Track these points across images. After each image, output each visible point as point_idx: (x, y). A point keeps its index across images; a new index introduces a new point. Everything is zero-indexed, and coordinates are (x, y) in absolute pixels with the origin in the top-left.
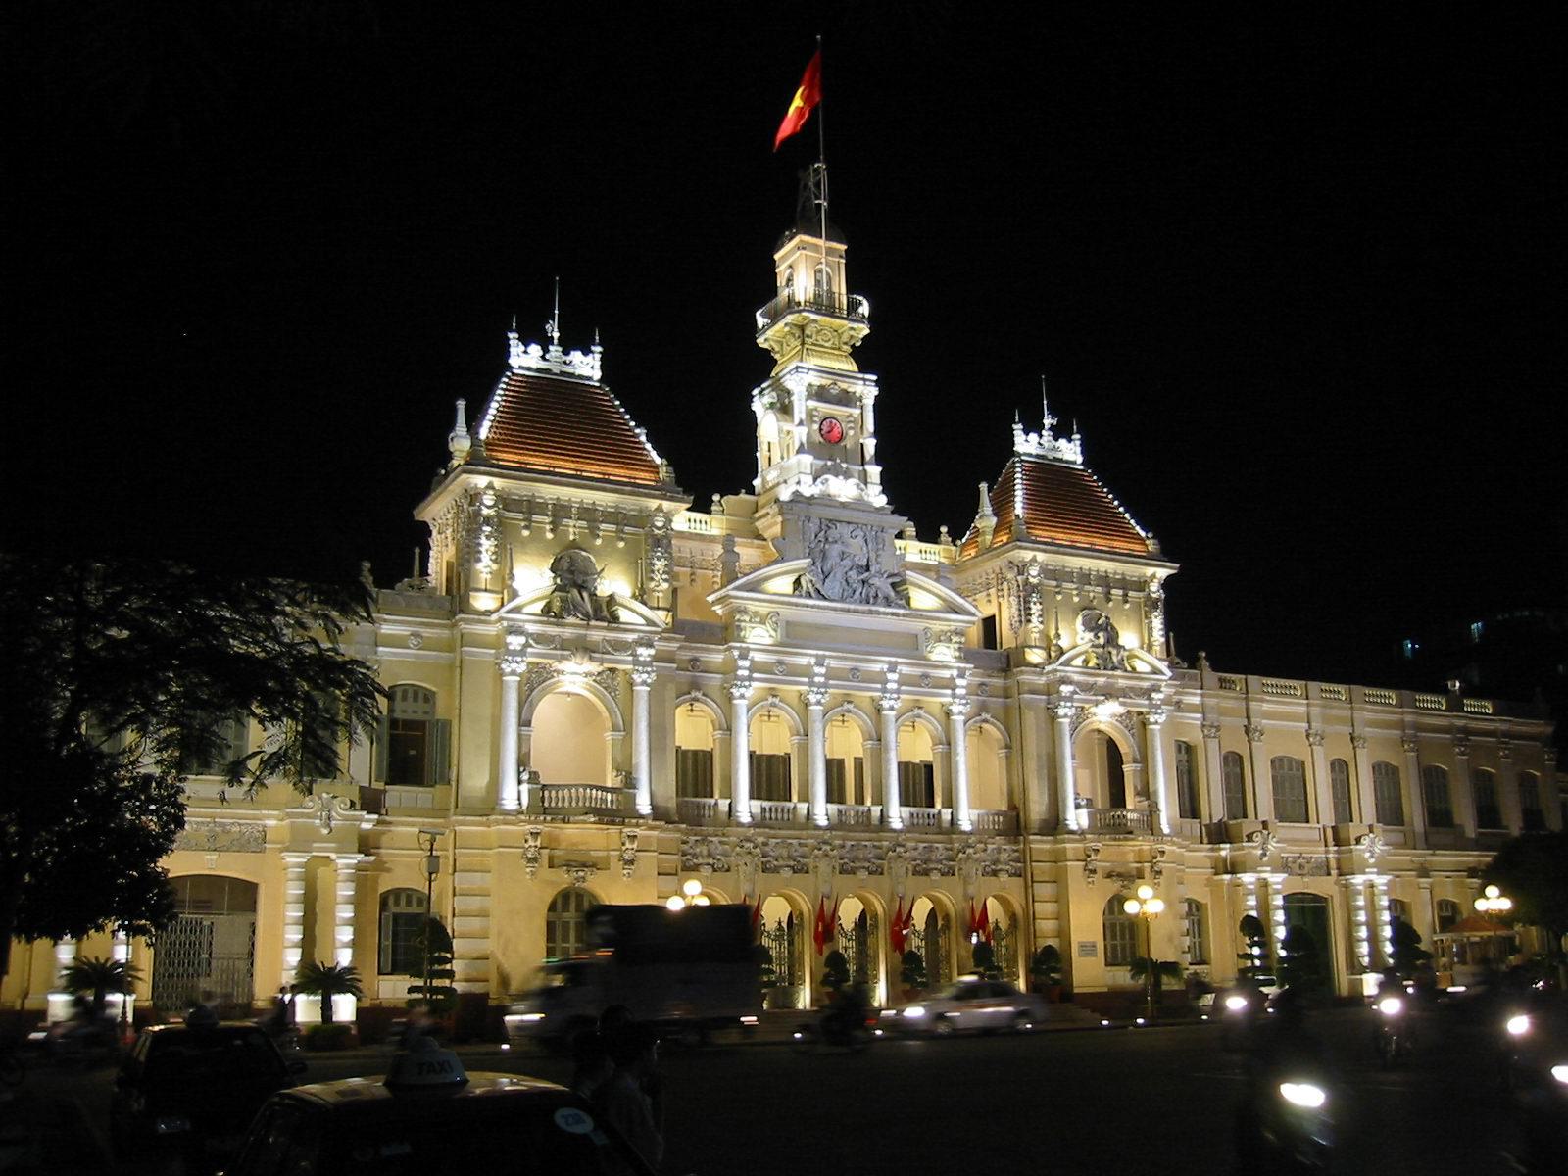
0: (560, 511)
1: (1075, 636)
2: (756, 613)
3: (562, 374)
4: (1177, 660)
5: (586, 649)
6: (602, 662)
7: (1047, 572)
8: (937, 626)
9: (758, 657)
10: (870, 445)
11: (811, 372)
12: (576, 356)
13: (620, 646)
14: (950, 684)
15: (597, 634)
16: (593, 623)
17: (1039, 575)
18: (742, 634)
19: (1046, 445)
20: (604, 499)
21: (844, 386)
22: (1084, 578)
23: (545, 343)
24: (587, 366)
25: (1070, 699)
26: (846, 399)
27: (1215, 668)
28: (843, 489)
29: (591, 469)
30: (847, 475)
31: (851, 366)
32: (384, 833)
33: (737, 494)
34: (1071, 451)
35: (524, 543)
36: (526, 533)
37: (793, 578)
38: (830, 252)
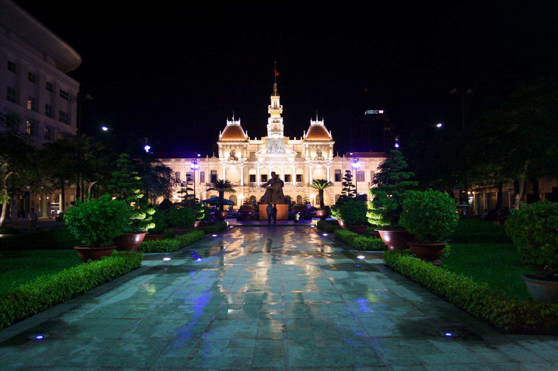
0: (231, 146)
5: (234, 164)
7: (309, 145)
10: (282, 129)
12: (236, 122)
15: (235, 162)
20: (237, 144)
22: (317, 145)
23: (232, 120)
24: (238, 123)
26: (278, 122)
28: (276, 136)
29: (235, 140)
31: (280, 116)
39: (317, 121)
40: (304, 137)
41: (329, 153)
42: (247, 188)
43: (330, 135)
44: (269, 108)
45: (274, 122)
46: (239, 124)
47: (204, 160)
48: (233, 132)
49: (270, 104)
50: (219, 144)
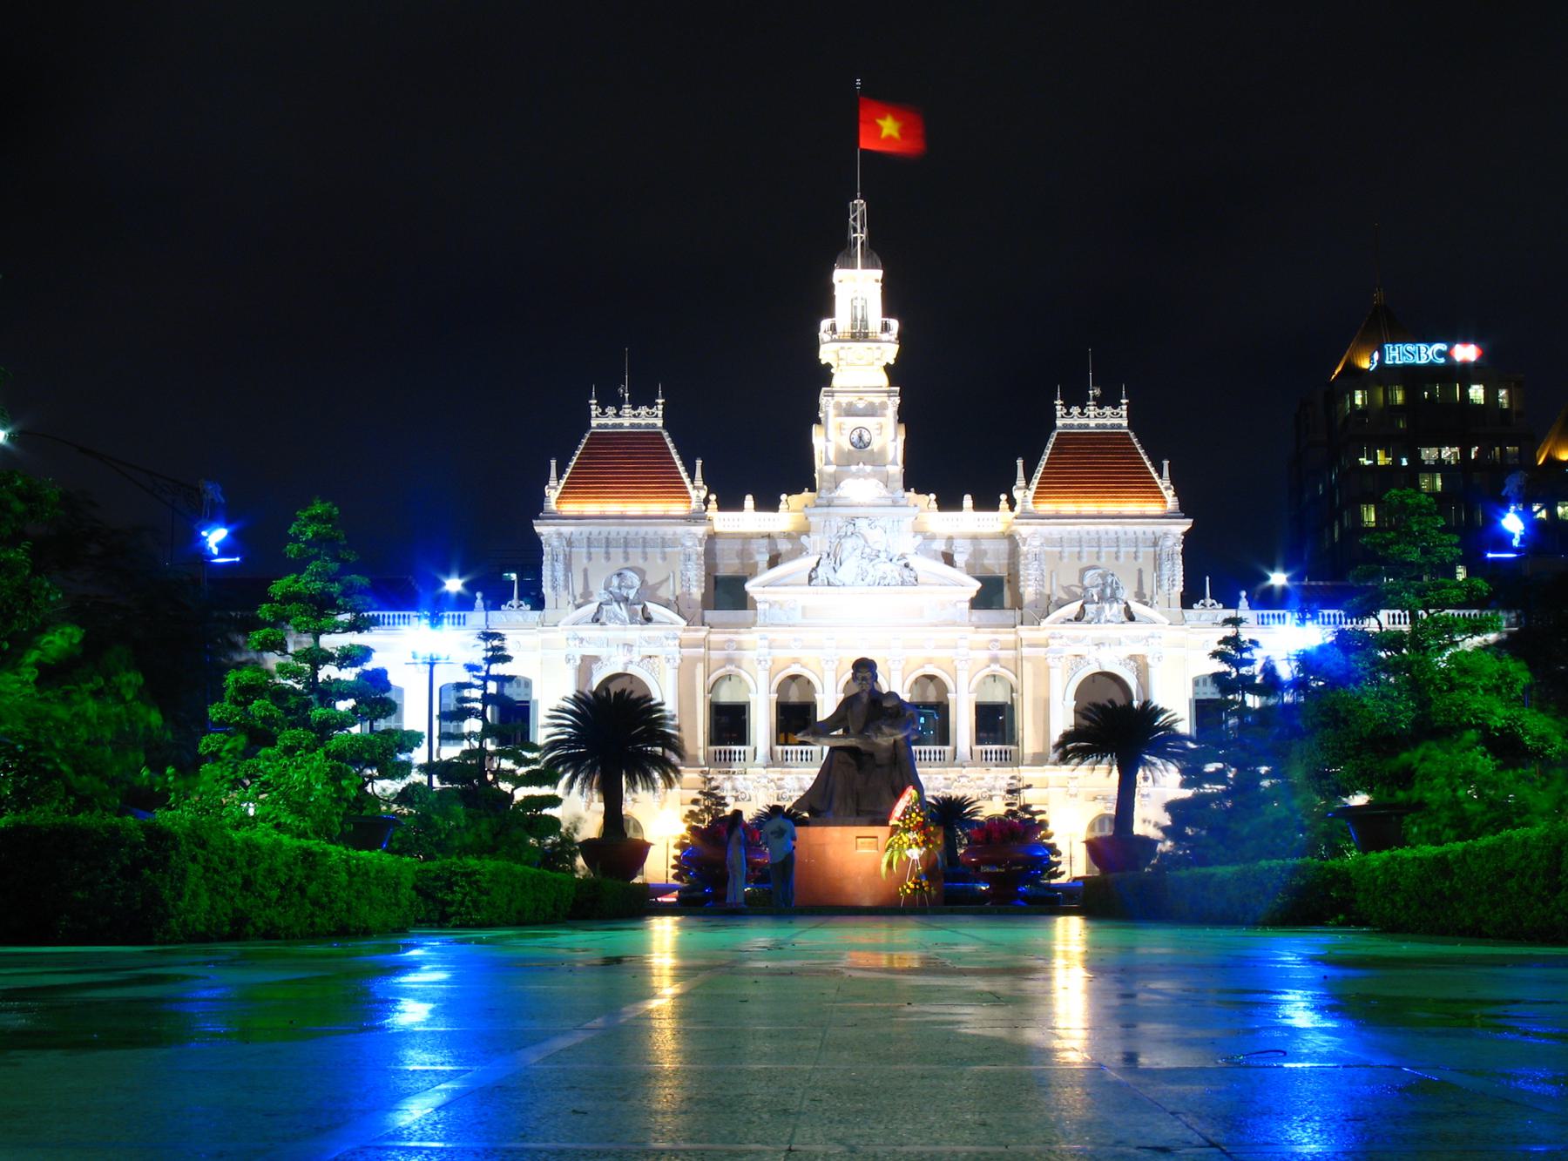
4: (1209, 601)
7: (1048, 541)
12: (643, 410)
19: (1092, 414)
24: (651, 418)
26: (871, 411)
27: (1251, 607)
30: (866, 476)
31: (883, 380)
33: (799, 491)
40: (1018, 494)
43: (1164, 484)
44: (824, 335)
45: (850, 411)
46: (660, 423)
48: (628, 466)
50: (541, 528)
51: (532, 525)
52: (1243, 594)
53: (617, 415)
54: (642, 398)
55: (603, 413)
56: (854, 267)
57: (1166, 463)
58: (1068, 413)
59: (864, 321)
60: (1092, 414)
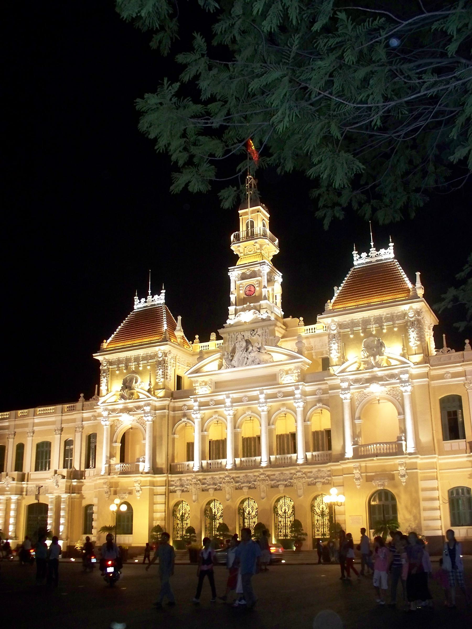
0: (128, 361)
1: (356, 355)
2: (203, 381)
3: (152, 305)
4: (445, 349)
6: (133, 415)
7: (341, 326)
8: (286, 368)
9: (203, 400)
11: (235, 270)
13: (139, 408)
14: (291, 394)
16: (128, 401)
17: (415, 316)
18: (197, 391)
20: (141, 352)
21: (253, 269)
25: (348, 389)
29: (137, 341)
32: (83, 486)
34: (388, 254)
35: (117, 376)
36: (117, 372)
37: (217, 363)
38: (253, 212)
39: (373, 250)
41: (406, 340)
42: (160, 478)
45: (244, 277)
47: (72, 409)
49: (237, 228)
51: (93, 356)
52: (467, 341)
53: (146, 302)
54: (156, 292)
55: (140, 302)
56: (247, 208)
57: (418, 274)
58: (360, 257)
59: (252, 232)
60: (374, 255)
